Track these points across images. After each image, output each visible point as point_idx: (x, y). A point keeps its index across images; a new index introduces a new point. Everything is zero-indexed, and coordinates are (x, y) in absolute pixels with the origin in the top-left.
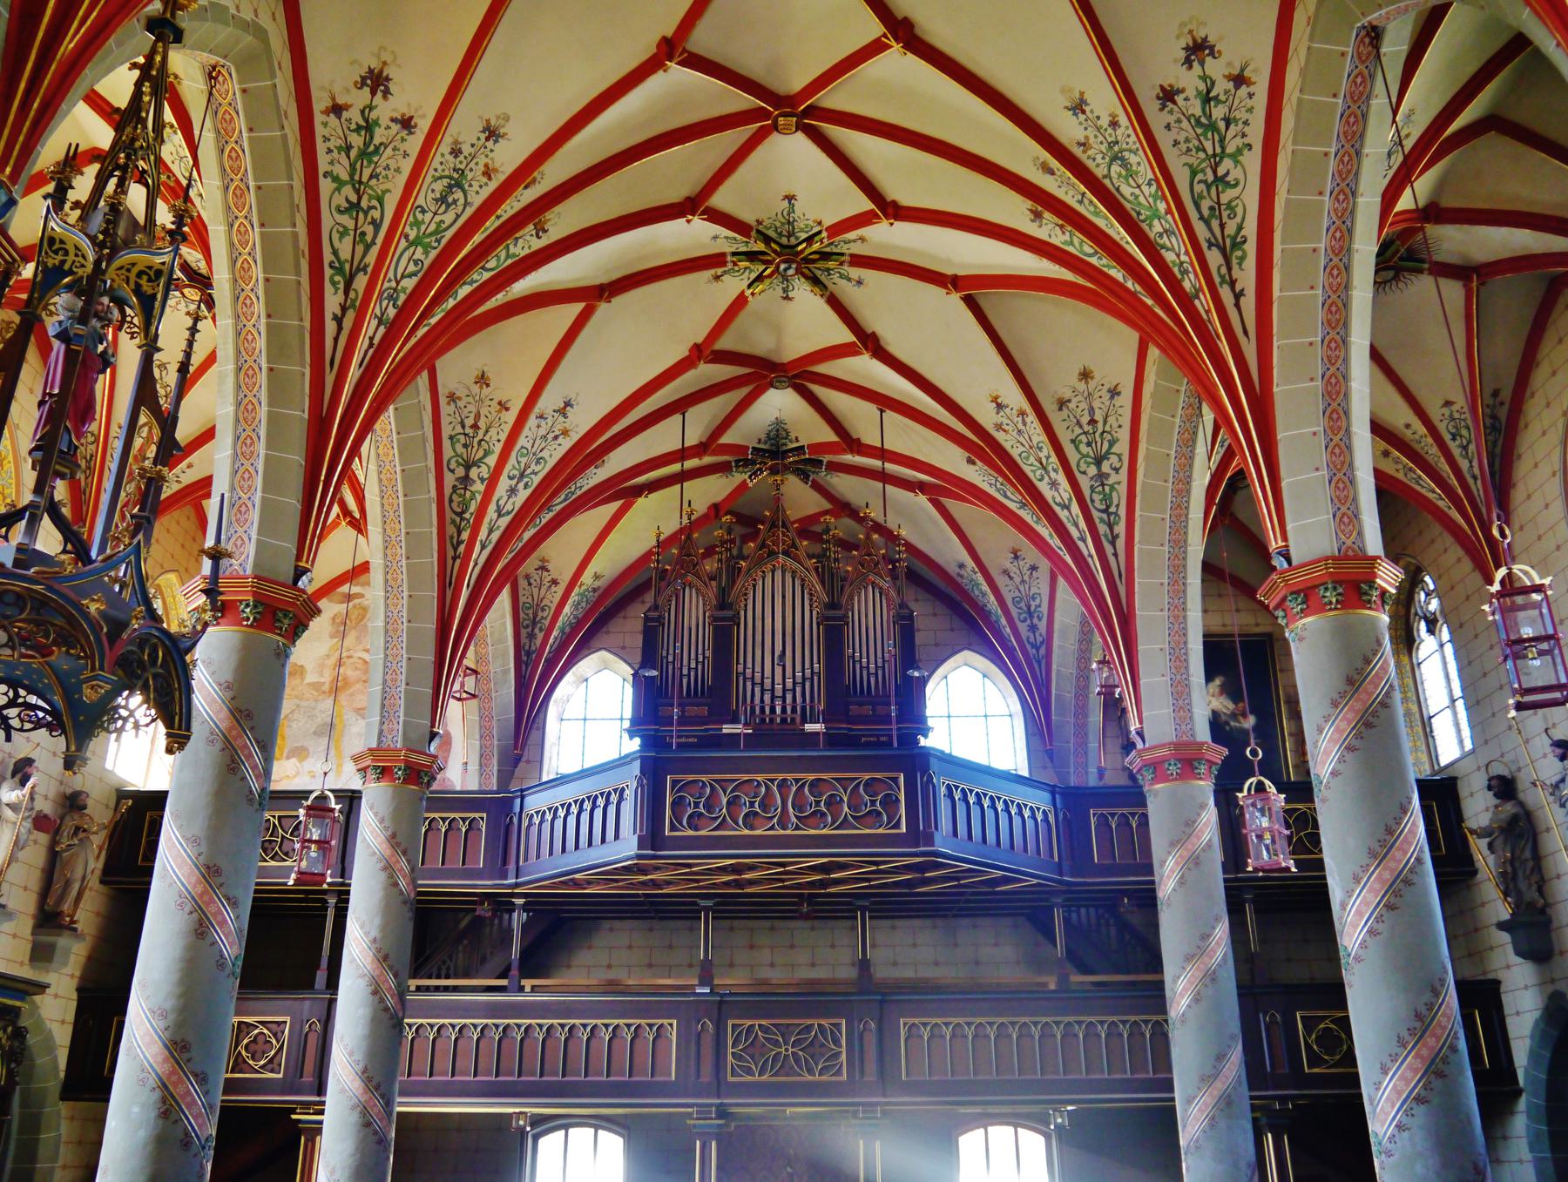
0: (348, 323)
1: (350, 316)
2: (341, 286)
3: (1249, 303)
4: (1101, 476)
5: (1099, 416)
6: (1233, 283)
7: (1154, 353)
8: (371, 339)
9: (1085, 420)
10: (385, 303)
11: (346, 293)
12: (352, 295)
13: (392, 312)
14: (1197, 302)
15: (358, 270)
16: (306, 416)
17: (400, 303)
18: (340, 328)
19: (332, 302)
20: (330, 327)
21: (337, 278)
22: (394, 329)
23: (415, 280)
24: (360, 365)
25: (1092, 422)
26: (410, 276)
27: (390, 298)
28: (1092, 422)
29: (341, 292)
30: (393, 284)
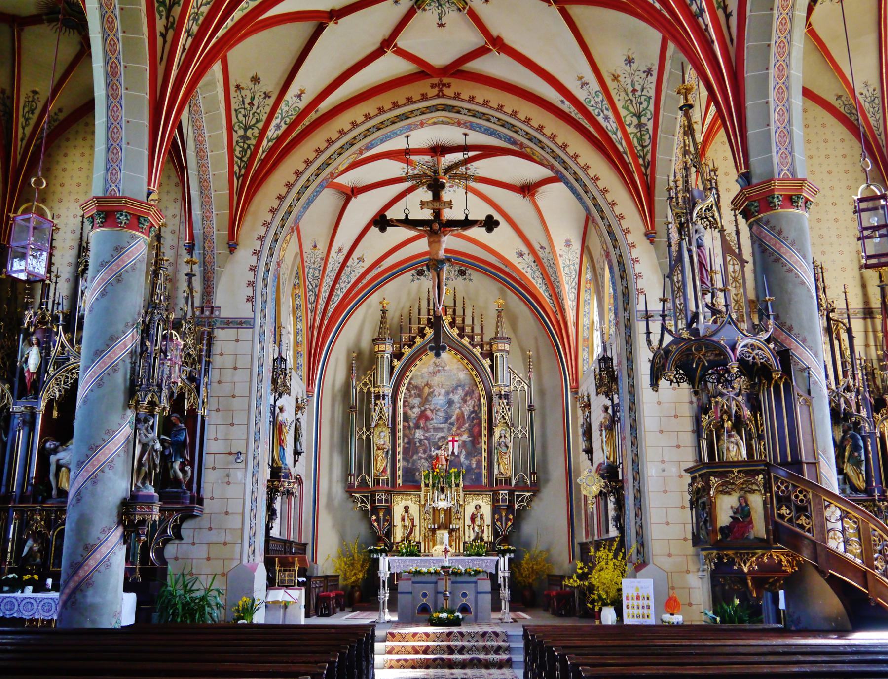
0: (169, 37)
1: (171, 33)
2: (164, 13)
3: (734, 21)
4: (640, 126)
5: (638, 87)
6: (725, 8)
7: (671, 47)
8: (184, 46)
9: (630, 89)
10: (191, 22)
11: (167, 18)
12: (171, 19)
13: (195, 29)
14: (700, 19)
15: (174, 4)
16: (148, 97)
17: (200, 22)
18: (165, 42)
19: (160, 24)
20: (160, 40)
21: (161, 9)
22: (197, 39)
23: (209, 7)
24: (178, 66)
25: (634, 91)
26: (206, 5)
27: (195, 19)
28: (634, 91)
29: (164, 17)
30: (196, 10)
